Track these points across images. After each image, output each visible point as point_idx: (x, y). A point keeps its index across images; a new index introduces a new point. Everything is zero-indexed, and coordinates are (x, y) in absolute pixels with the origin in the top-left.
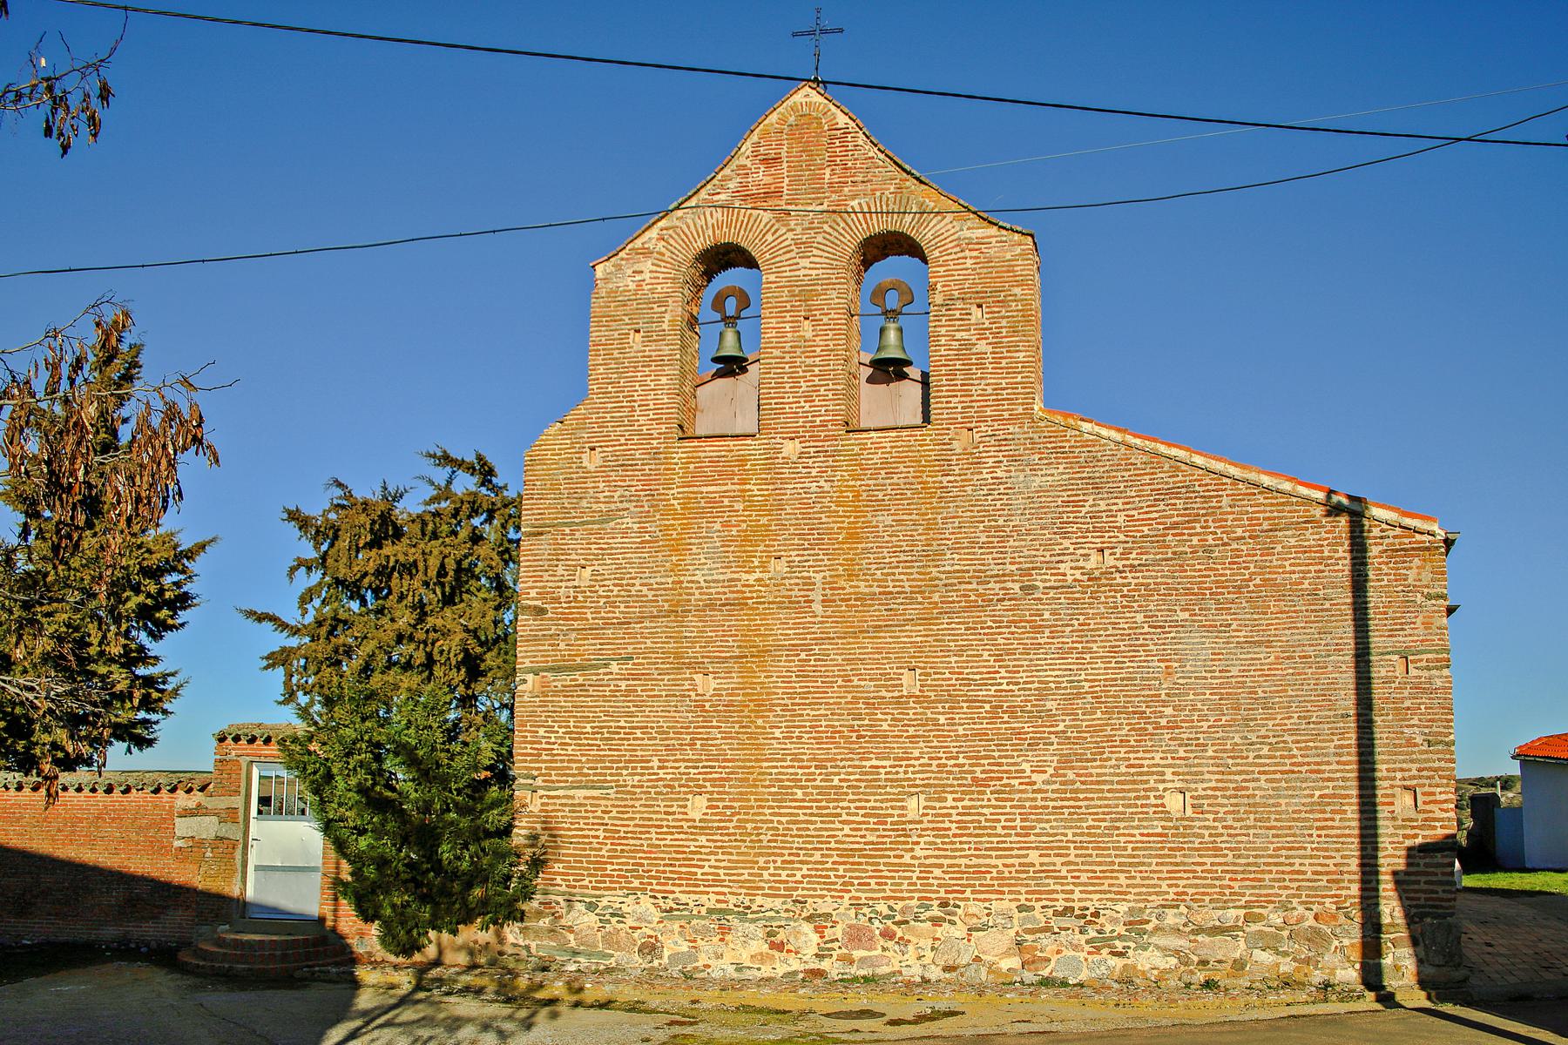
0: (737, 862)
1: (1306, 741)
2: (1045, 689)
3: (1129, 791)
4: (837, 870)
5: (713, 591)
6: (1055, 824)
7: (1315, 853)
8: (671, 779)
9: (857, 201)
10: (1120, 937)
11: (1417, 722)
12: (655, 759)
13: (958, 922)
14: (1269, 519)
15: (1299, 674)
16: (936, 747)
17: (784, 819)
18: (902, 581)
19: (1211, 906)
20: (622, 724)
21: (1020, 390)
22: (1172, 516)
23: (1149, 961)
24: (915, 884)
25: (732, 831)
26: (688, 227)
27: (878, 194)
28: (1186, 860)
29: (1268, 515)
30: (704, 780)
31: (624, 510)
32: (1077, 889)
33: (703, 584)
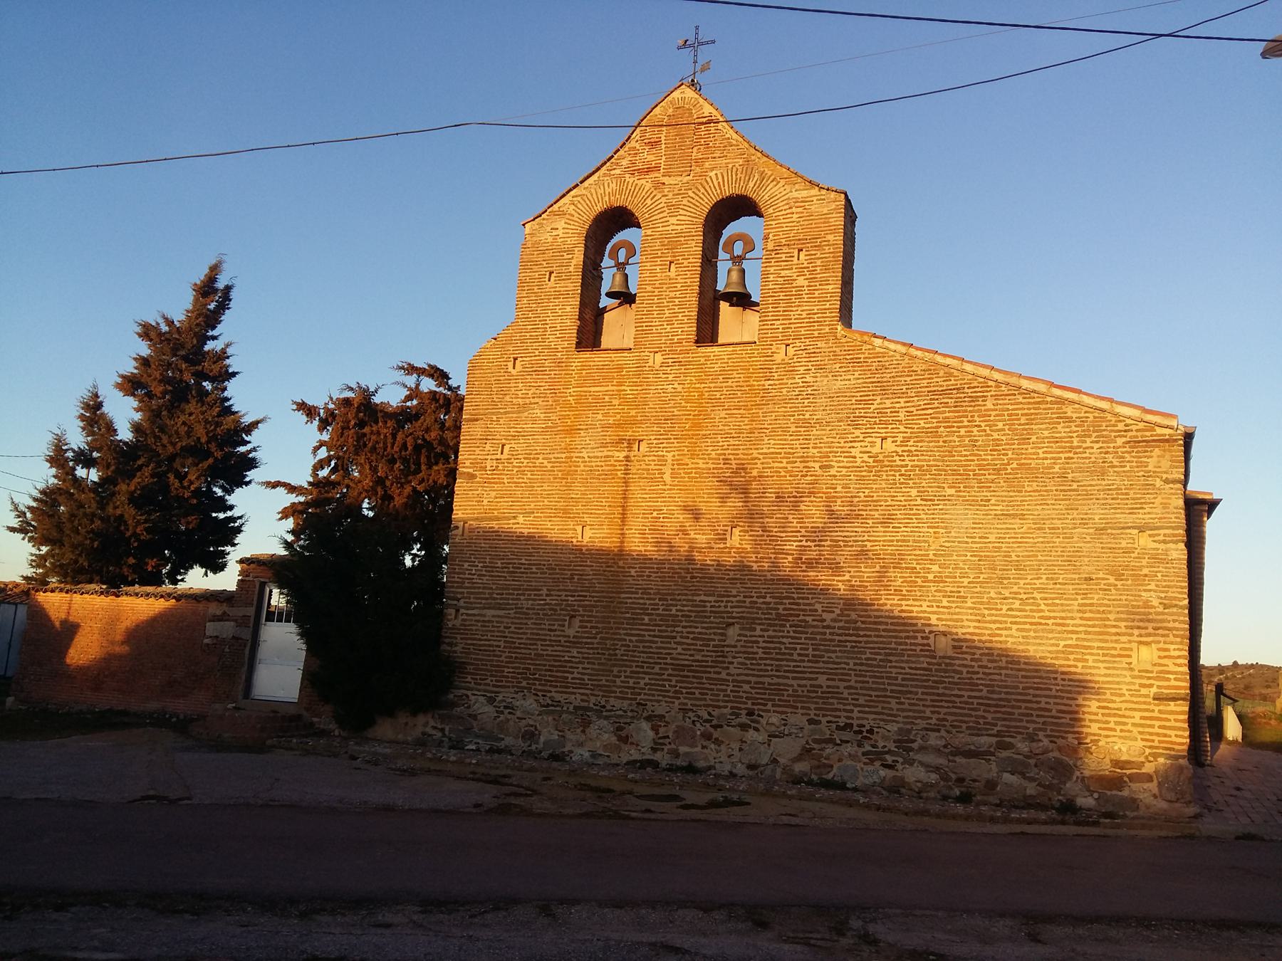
0: (599, 670)
1: (1053, 599)
2: (835, 546)
3: (901, 631)
4: (671, 681)
5: (593, 464)
6: (840, 654)
7: (1060, 694)
8: (556, 604)
9: (714, 172)
10: (889, 752)
11: (1154, 588)
12: (545, 589)
13: (761, 729)
14: (1026, 414)
15: (1048, 542)
16: (749, 588)
17: (634, 639)
18: (730, 459)
19: (968, 732)
20: (523, 561)
21: (828, 315)
22: (945, 412)
23: (914, 774)
24: (729, 696)
25: (595, 646)
26: (592, 195)
27: (730, 166)
28: (947, 692)
29: (1026, 411)
30: (579, 606)
31: (535, 403)
32: (856, 710)
33: (587, 459)
